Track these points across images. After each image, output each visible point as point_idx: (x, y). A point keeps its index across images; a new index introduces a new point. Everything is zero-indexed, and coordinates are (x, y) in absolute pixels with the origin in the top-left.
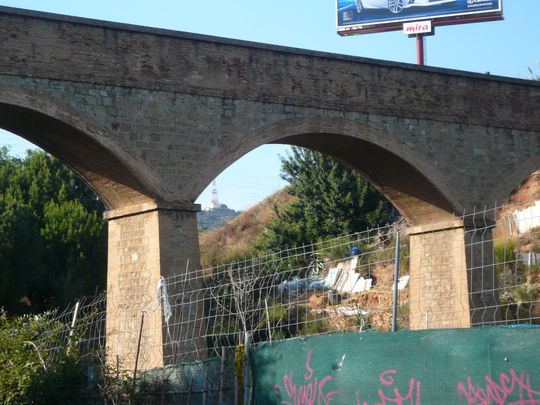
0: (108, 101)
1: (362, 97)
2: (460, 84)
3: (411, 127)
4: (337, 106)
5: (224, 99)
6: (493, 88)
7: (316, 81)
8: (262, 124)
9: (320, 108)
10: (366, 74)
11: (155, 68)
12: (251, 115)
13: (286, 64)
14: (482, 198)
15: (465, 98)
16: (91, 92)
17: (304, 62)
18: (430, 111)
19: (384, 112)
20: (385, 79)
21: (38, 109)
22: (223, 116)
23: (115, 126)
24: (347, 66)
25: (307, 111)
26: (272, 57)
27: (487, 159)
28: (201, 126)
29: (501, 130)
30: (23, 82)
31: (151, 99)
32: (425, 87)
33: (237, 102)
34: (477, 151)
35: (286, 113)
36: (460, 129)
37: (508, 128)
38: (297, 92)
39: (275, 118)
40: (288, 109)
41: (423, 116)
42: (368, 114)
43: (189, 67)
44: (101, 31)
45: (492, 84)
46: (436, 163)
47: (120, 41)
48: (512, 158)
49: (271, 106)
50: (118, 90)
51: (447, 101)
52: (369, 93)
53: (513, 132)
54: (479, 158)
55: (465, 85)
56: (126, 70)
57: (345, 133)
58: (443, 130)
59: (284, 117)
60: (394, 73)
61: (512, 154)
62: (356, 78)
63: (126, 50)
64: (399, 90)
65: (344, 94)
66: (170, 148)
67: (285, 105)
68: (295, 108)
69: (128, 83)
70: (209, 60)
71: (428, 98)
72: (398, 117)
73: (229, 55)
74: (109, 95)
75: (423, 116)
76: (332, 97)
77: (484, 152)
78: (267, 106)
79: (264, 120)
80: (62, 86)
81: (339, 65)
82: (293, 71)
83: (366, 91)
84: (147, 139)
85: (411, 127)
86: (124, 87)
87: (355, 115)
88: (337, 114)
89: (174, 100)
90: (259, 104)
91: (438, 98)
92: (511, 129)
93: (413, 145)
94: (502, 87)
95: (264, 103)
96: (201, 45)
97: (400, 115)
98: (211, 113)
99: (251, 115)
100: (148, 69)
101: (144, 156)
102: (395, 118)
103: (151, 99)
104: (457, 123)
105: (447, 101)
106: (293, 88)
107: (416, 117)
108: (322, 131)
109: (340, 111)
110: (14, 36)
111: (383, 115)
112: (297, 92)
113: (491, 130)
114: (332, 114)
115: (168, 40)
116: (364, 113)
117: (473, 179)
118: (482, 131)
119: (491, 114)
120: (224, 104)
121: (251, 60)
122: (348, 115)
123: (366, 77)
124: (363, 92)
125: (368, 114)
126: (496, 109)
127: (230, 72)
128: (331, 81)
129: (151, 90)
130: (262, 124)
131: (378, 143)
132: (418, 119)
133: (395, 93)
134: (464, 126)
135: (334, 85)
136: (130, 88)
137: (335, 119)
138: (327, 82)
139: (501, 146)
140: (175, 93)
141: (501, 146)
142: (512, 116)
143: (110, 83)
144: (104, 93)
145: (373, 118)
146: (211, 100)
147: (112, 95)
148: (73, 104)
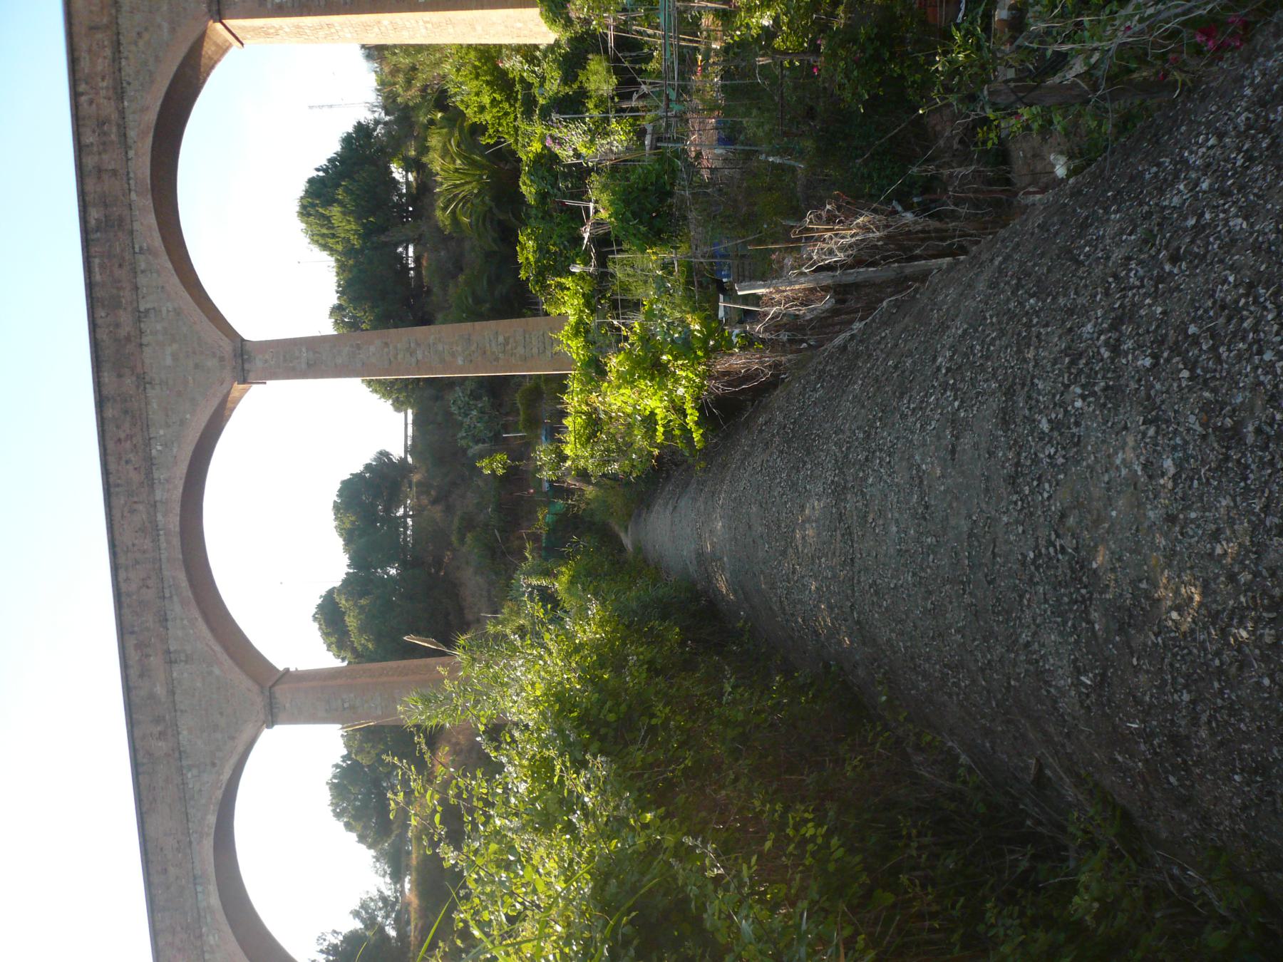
0: (195, 771)
1: (141, 507)
2: (106, 380)
3: (159, 448)
4: (155, 540)
5: (171, 662)
6: (103, 335)
7: (137, 562)
8: (185, 622)
9: (160, 559)
10: (120, 501)
11: (159, 729)
12: (180, 633)
13: (129, 595)
14: (214, 355)
15: (120, 376)
16: (190, 786)
17: (122, 575)
18: (139, 423)
19: (150, 483)
20: (119, 478)
21: (213, 830)
22: (186, 662)
23: (214, 765)
24: (116, 527)
25: (166, 573)
26: (125, 611)
27: (175, 346)
28: (199, 684)
29: (142, 325)
30: (194, 844)
31: (185, 732)
32: (118, 427)
33: (172, 649)
34: (169, 361)
35: (171, 597)
36: (150, 383)
37: (140, 316)
38: (150, 583)
39: (178, 608)
40: (167, 595)
41: (146, 433)
42: (155, 502)
43: (152, 696)
44: (141, 777)
45: (98, 336)
46: (188, 416)
47: (145, 761)
48: (168, 311)
49: (168, 613)
50: (184, 763)
51: (126, 401)
52: (135, 499)
53: (142, 309)
54: (175, 357)
55: (106, 374)
56: (167, 755)
57: (178, 529)
58: (155, 406)
59: (175, 598)
60: (112, 467)
61: (164, 310)
62: (125, 514)
63: (151, 755)
64: (127, 462)
65: (143, 530)
66: (221, 714)
67: (164, 597)
68: (166, 585)
69: (177, 755)
70: (141, 676)
71: (127, 425)
72: (152, 464)
73: (134, 656)
74: (190, 770)
75: (146, 433)
76: (147, 544)
77: (169, 350)
78: (169, 617)
79: (182, 619)
80: (191, 811)
81: (116, 533)
82: (134, 587)
83: (135, 502)
84: (219, 736)
85: (159, 448)
86: (180, 759)
87: (159, 517)
88: (162, 538)
89: (182, 711)
90: (170, 624)
91: (126, 412)
92: (139, 312)
93: (175, 445)
94: (99, 321)
95: (166, 620)
96: (131, 684)
97: (150, 462)
98: (186, 675)
99: (180, 633)
100: (162, 735)
101: (232, 738)
102: (154, 468)
103: (185, 732)
104: (145, 388)
105: (126, 401)
106: (148, 587)
107: (148, 442)
108: (181, 556)
109: (158, 535)
110: (162, 849)
111: (153, 484)
112: (150, 583)
113: (145, 340)
114: (164, 545)
115: (134, 716)
116: (156, 506)
117: (197, 366)
118: (147, 350)
119: (128, 339)
120: (176, 662)
121: (132, 633)
122: (160, 527)
123: (122, 502)
124: (136, 506)
125: (155, 502)
126: (123, 332)
127: (148, 656)
128: (134, 545)
129: (179, 733)
130: (185, 622)
131: (181, 490)
132: (150, 439)
133: (130, 467)
134: (147, 379)
135: (136, 542)
136: (180, 753)
137: (168, 542)
138: (135, 549)
139: (159, 327)
140: (175, 711)
141: (159, 327)
142: (125, 309)
143: (180, 770)
144: (189, 775)
145: (159, 495)
146: (175, 675)
147: (190, 768)
148: (203, 801)
